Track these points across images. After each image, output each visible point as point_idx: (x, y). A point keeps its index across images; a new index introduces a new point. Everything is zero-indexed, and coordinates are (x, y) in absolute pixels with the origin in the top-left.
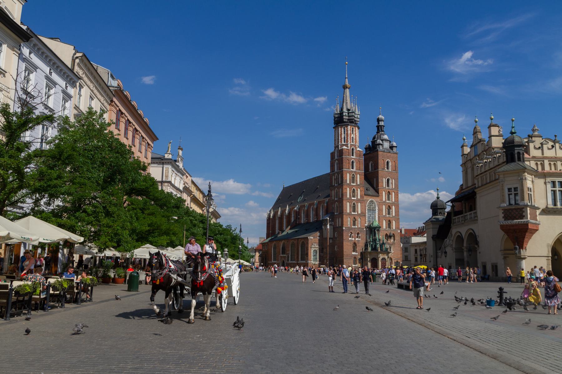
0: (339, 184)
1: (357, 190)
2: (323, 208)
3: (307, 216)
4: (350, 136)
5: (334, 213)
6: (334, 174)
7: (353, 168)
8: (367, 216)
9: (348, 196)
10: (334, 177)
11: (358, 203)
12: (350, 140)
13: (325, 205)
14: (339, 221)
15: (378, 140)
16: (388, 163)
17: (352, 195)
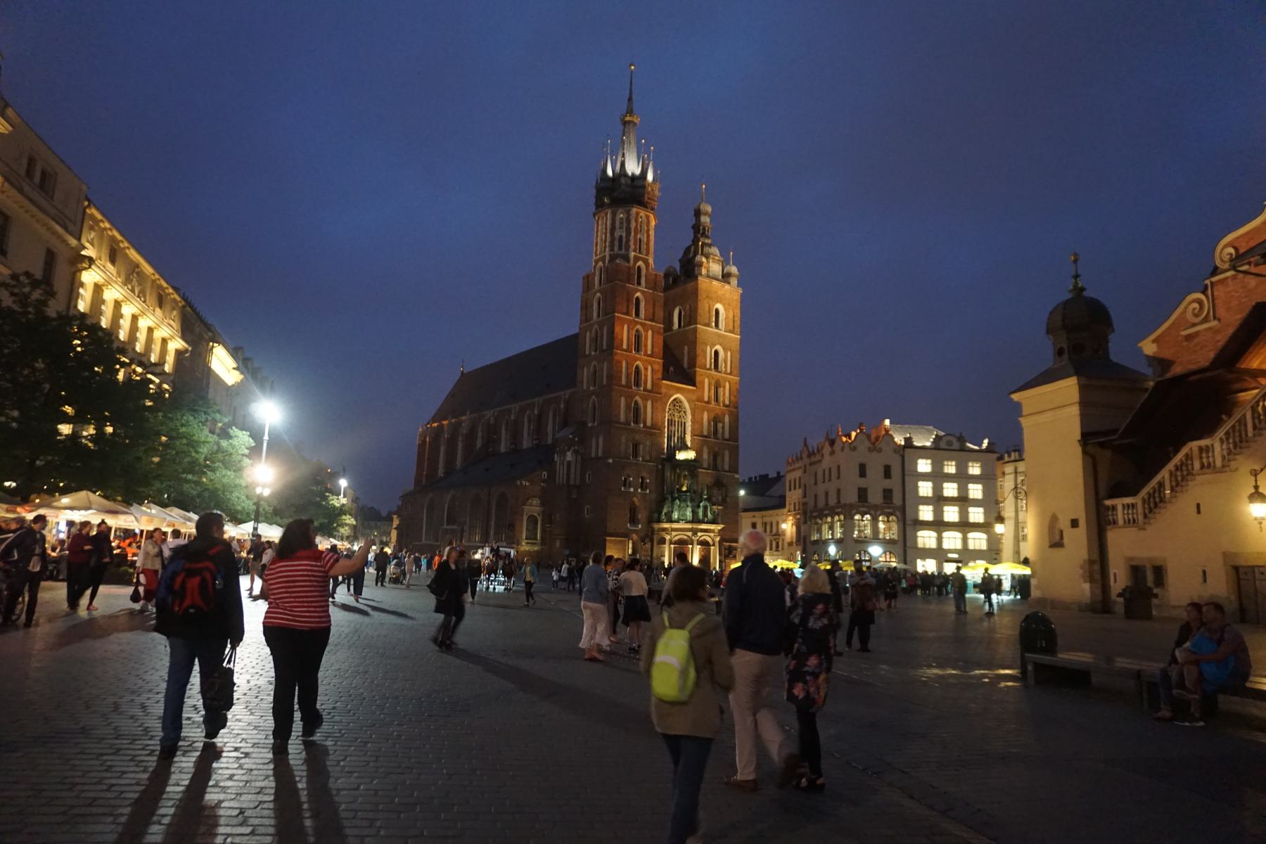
0: (603, 351)
1: (646, 369)
2: (554, 416)
3: (516, 436)
4: (636, 235)
5: (584, 424)
6: (592, 325)
7: (637, 314)
8: (666, 435)
9: (624, 382)
10: (591, 332)
11: (647, 400)
12: (635, 244)
13: (562, 406)
14: (597, 444)
15: (699, 256)
16: (717, 312)
17: (633, 380)
